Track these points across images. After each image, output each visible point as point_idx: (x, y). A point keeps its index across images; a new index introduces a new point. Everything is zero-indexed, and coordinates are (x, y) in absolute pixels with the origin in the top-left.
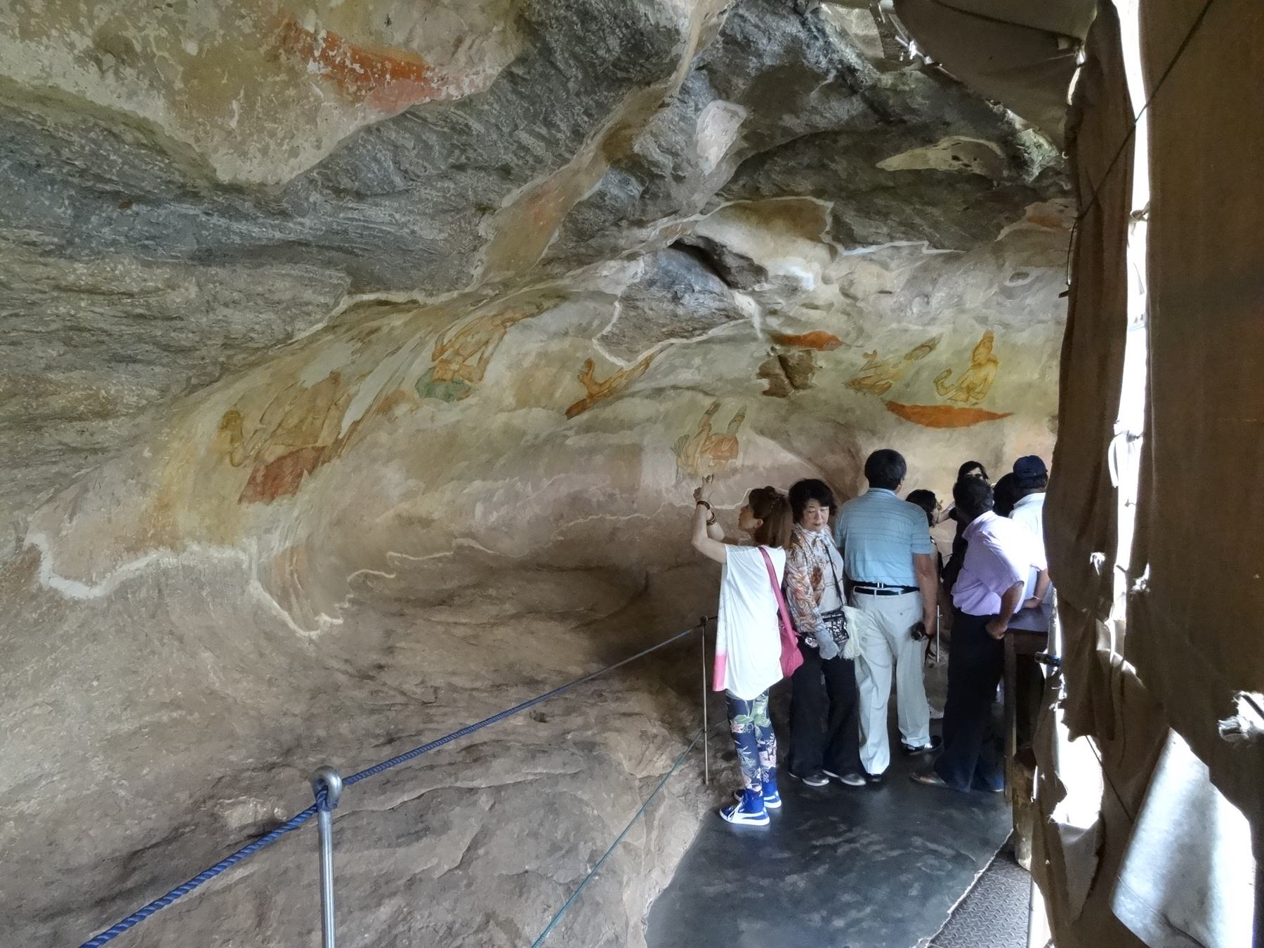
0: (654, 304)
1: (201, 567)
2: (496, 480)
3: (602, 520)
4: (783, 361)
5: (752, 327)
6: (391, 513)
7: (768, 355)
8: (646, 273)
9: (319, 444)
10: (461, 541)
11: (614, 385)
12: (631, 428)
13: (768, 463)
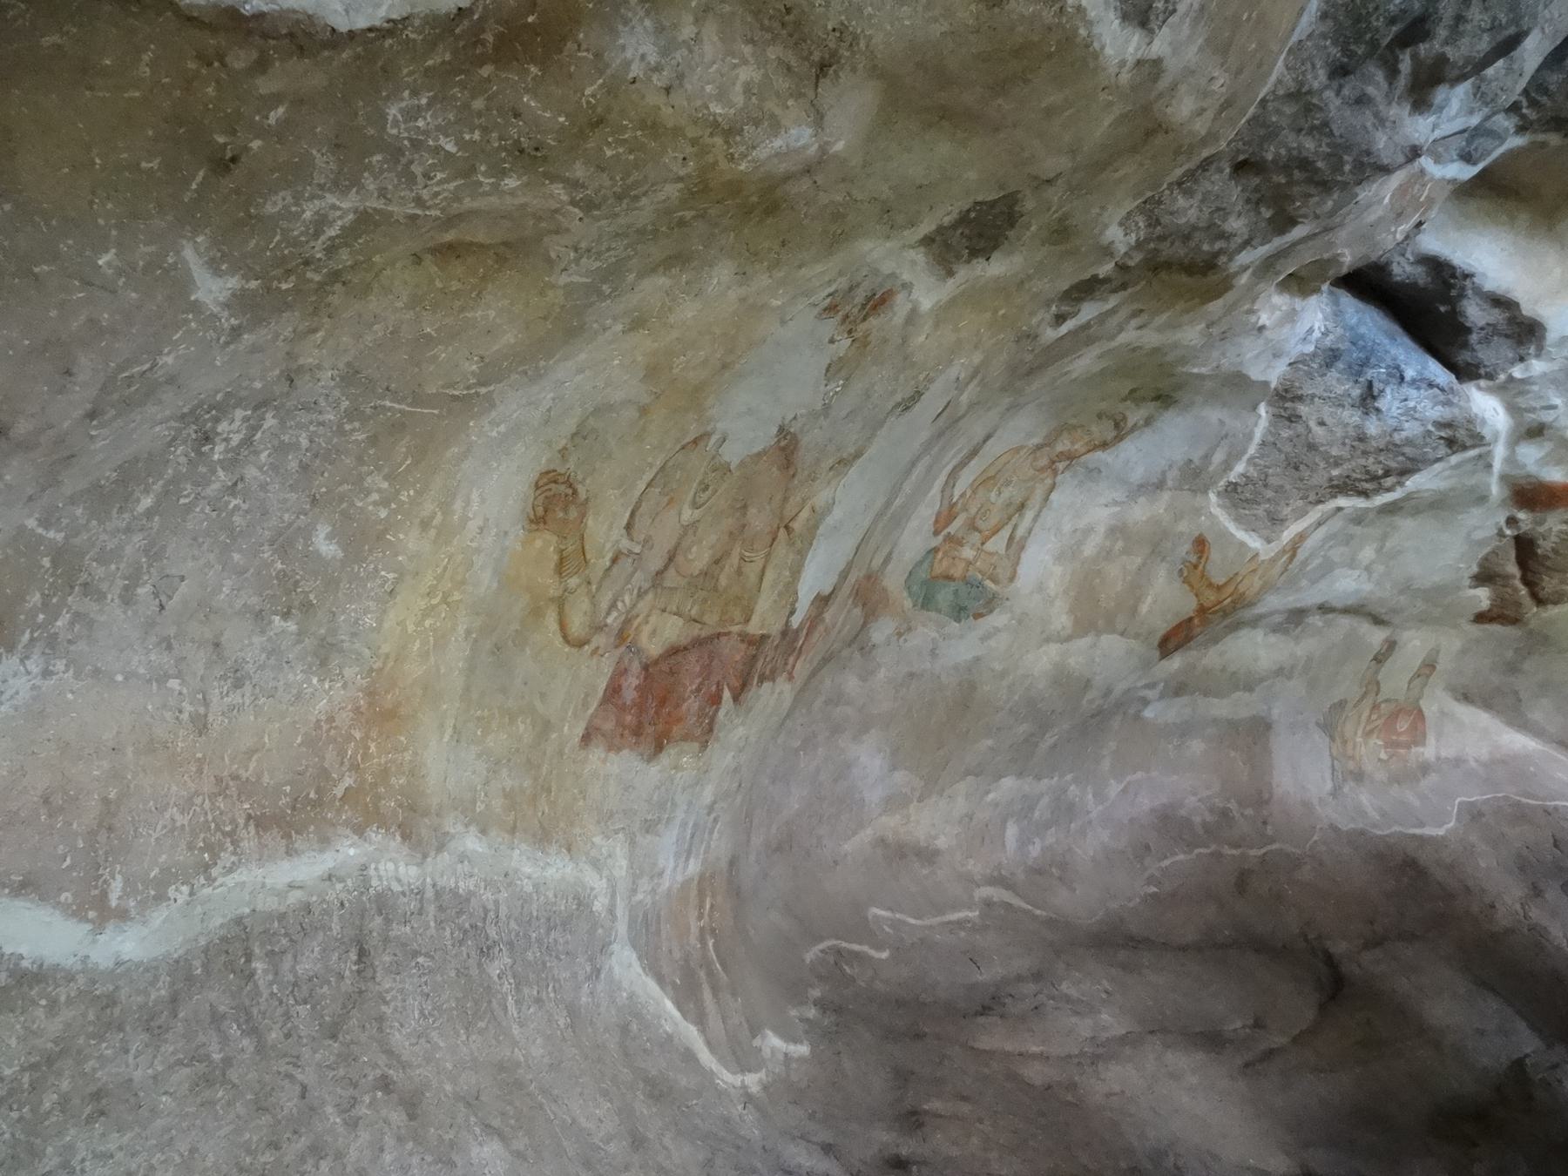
1: (488, 896)
2: (1038, 778)
3: (1217, 855)
4: (1525, 547)
5: (1489, 466)
6: (867, 834)
7: (1501, 534)
9: (754, 628)
10: (987, 891)
11: (1241, 589)
12: (1249, 688)
13: (1484, 753)
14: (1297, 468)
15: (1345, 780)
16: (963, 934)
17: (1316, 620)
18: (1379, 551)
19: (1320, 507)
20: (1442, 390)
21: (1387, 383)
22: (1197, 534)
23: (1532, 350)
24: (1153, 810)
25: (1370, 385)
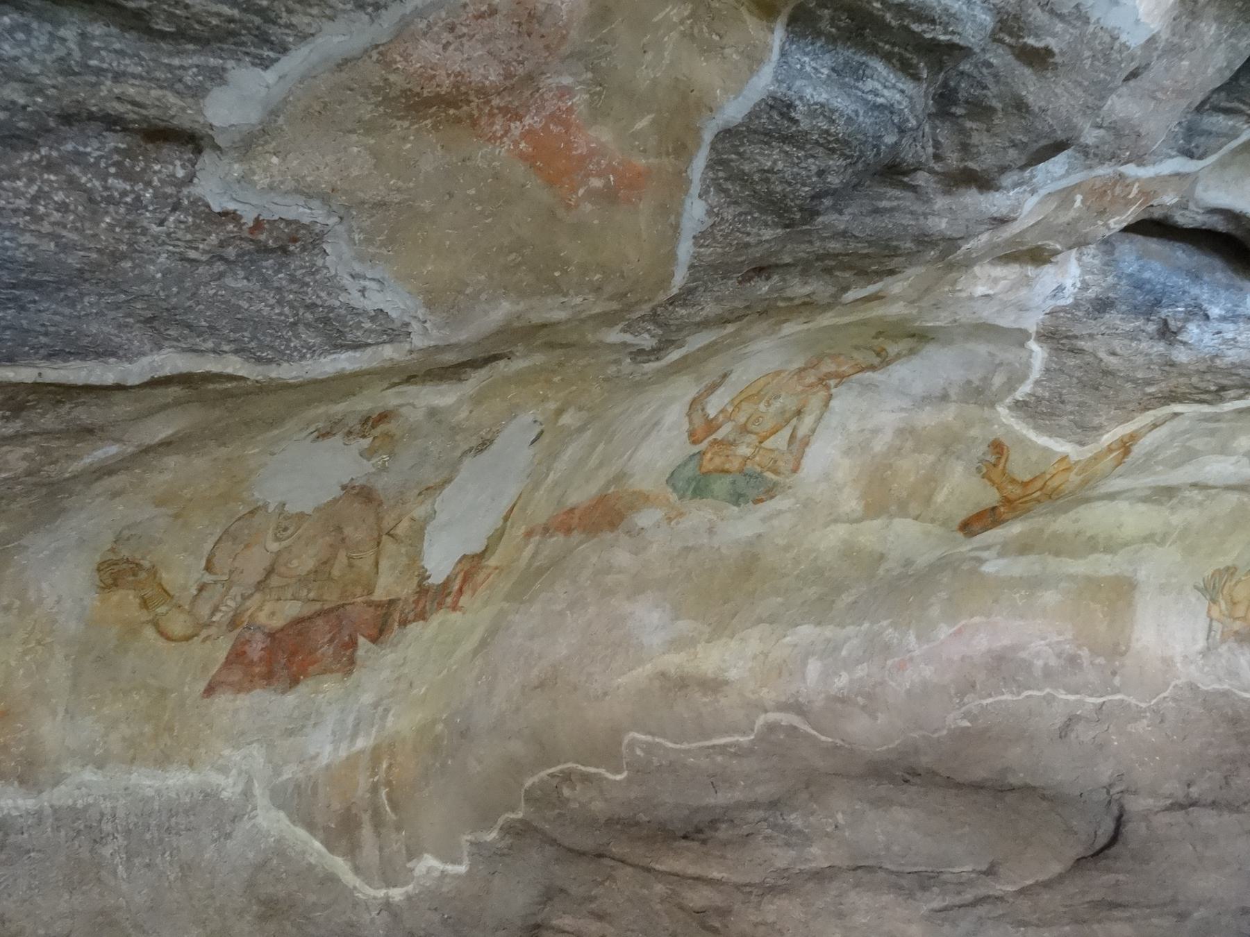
0: (1117, 345)
2: (842, 625)
6: (643, 672)
8: (1085, 286)
9: (379, 595)
10: (773, 716)
11: (1055, 482)
14: (1097, 389)
15: (1223, 641)
16: (719, 759)
17: (1197, 495)
19: (1151, 412)
21: (1186, 320)
22: (992, 438)
24: (989, 651)
25: (1165, 322)
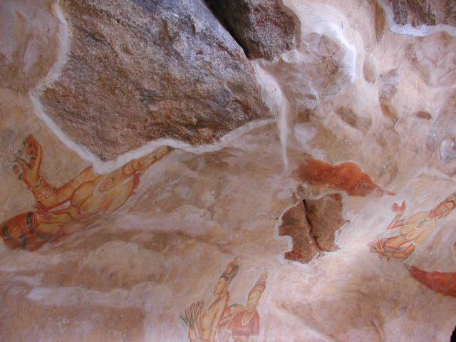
18: (217, 196)
19: (153, 143)
20: (231, 55)
22: (26, 134)
23: (294, 41)
